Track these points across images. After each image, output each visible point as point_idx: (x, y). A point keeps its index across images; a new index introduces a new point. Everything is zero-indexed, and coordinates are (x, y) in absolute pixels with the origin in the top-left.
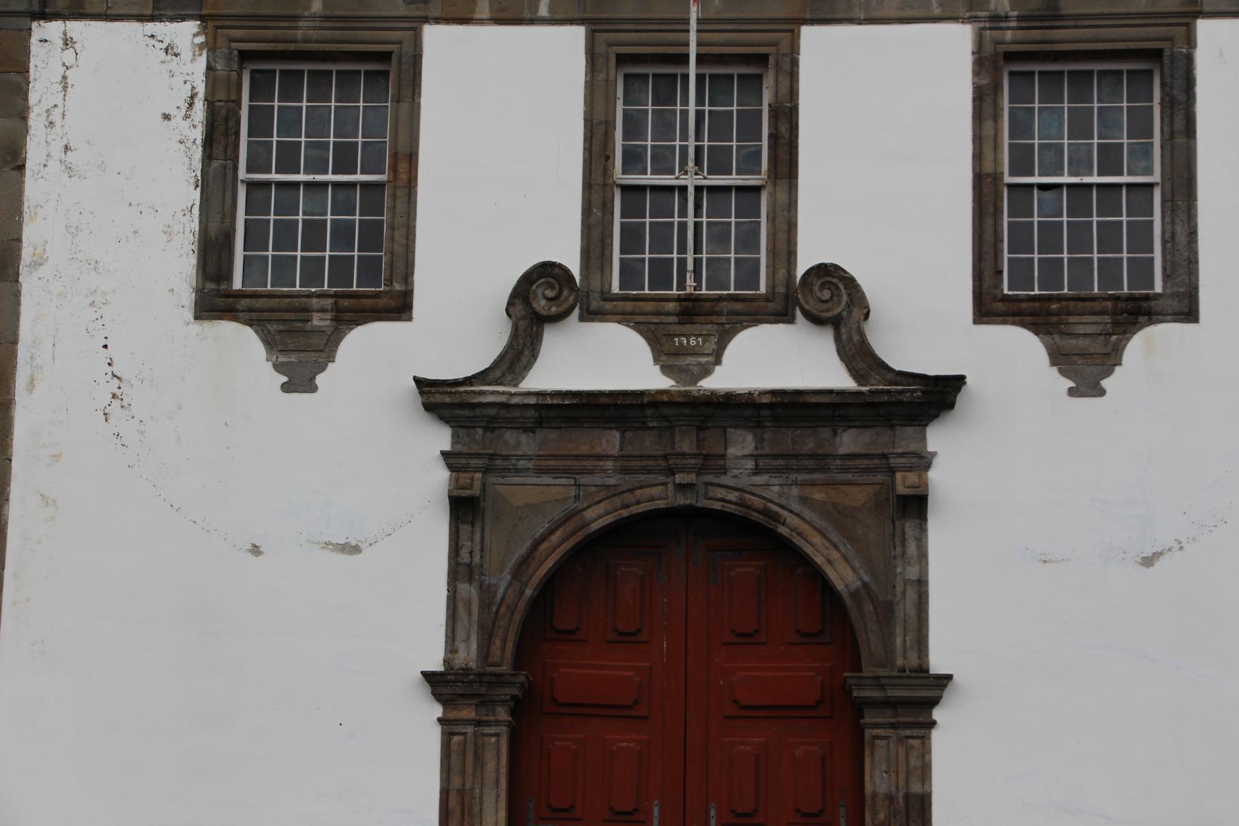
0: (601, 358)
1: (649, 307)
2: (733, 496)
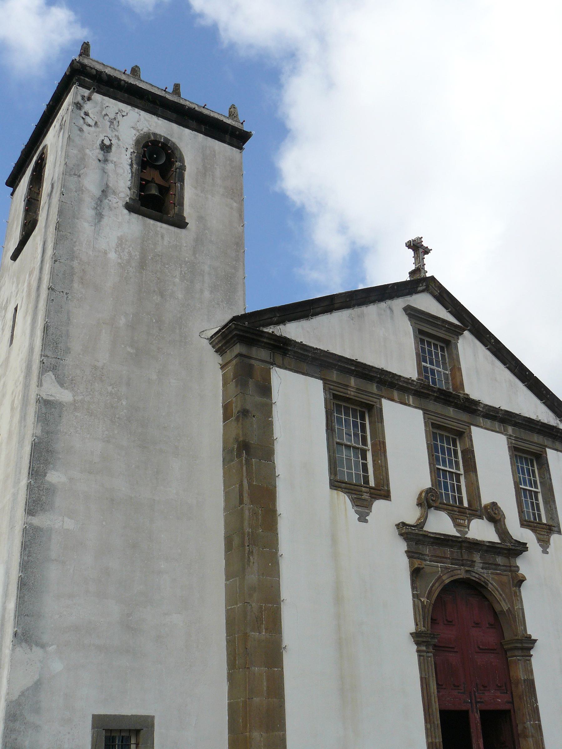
0: (441, 524)
1: (450, 508)
2: (477, 576)
